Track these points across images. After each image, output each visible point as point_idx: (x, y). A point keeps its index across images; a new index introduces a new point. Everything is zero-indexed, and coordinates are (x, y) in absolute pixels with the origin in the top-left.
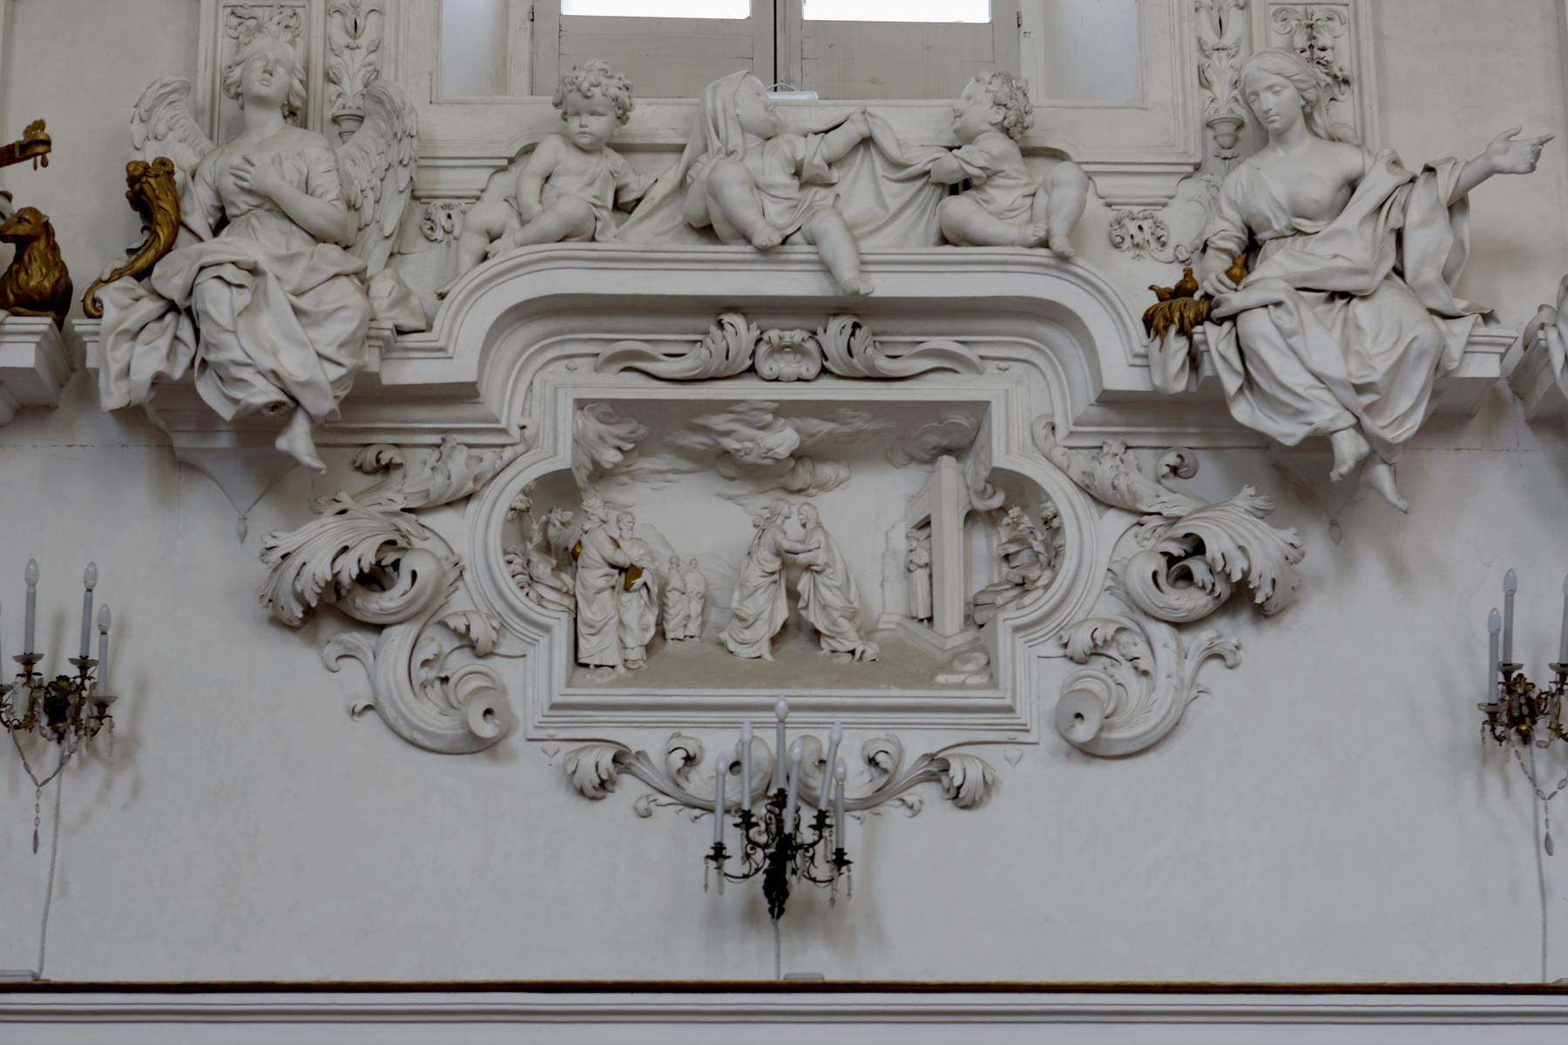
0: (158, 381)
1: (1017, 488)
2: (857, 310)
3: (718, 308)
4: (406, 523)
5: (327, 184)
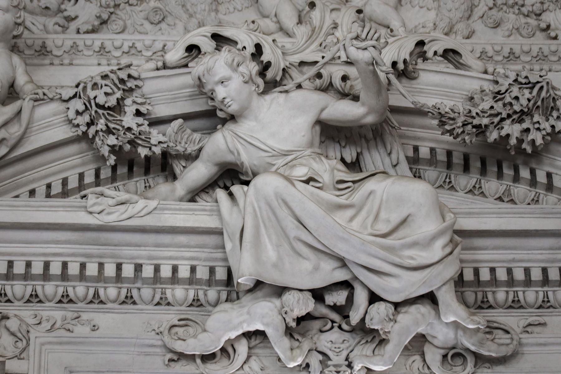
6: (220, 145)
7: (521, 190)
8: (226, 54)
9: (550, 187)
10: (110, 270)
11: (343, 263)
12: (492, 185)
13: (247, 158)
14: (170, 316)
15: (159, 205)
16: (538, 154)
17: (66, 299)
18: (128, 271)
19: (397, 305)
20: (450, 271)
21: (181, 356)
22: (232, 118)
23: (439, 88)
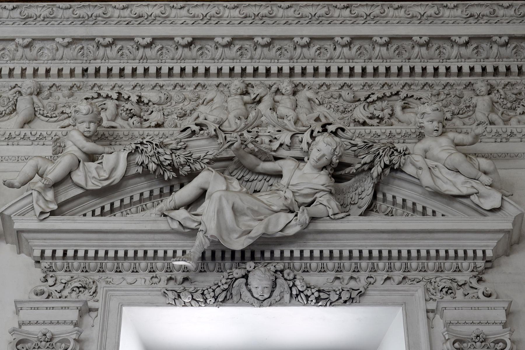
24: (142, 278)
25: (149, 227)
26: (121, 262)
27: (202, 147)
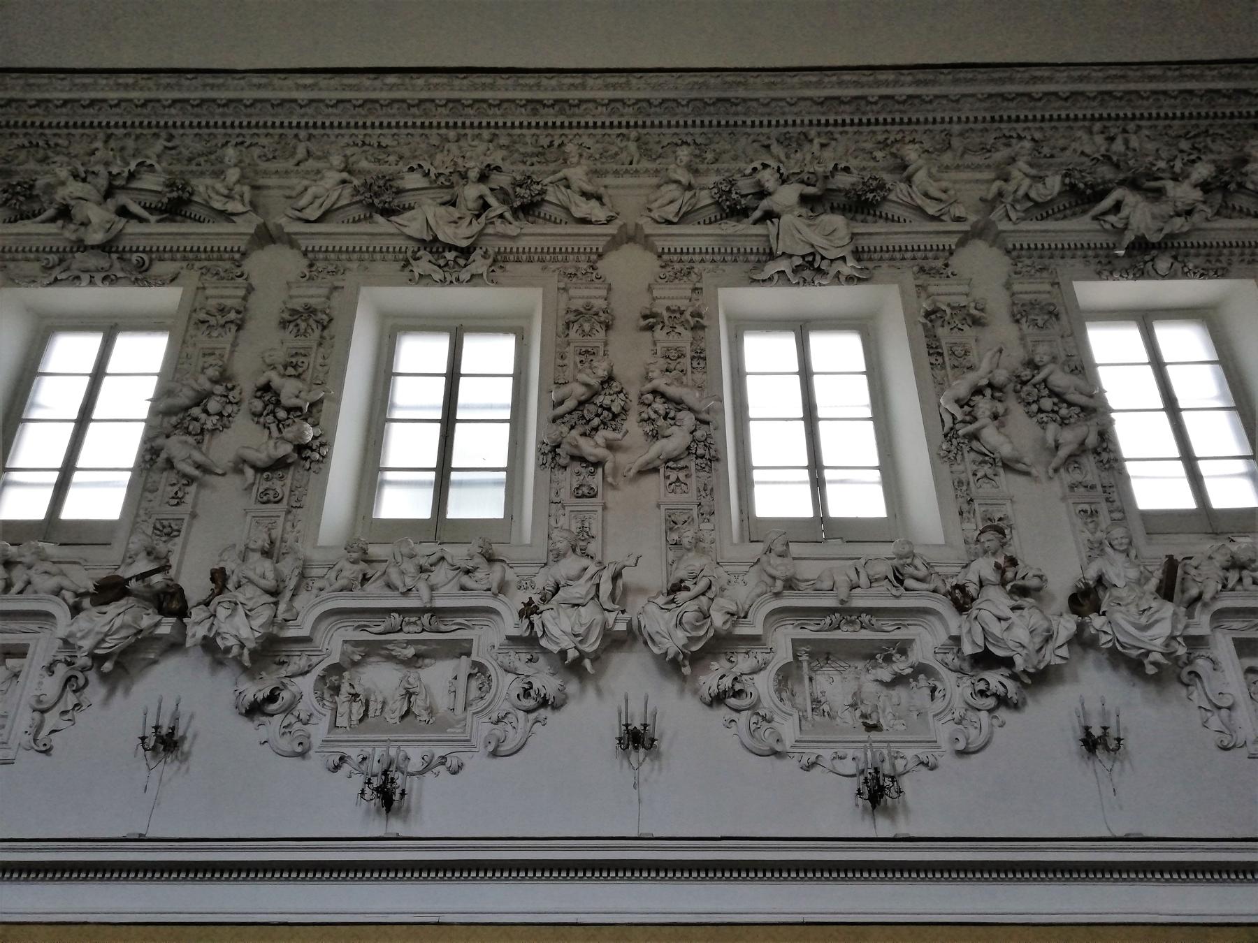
0: (205, 637)
1: (479, 668)
2: (435, 612)
3: (389, 611)
4: (286, 681)
5: (270, 575)
6: (765, 204)
7: (870, 218)
8: (768, 171)
9: (881, 217)
10: (729, 250)
11: (813, 246)
12: (859, 217)
13: (776, 209)
14: (750, 266)
15: (744, 227)
16: (878, 204)
17: (713, 261)
18: (735, 250)
19: (832, 261)
20: (851, 248)
21: (754, 281)
22: (770, 194)
23: (843, 181)
24: (1078, 264)
25: (1088, 227)
26: (1066, 251)
27: (1105, 172)
